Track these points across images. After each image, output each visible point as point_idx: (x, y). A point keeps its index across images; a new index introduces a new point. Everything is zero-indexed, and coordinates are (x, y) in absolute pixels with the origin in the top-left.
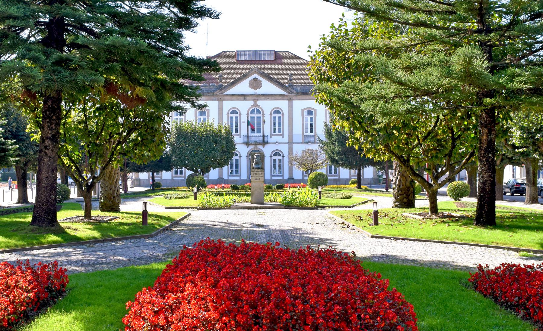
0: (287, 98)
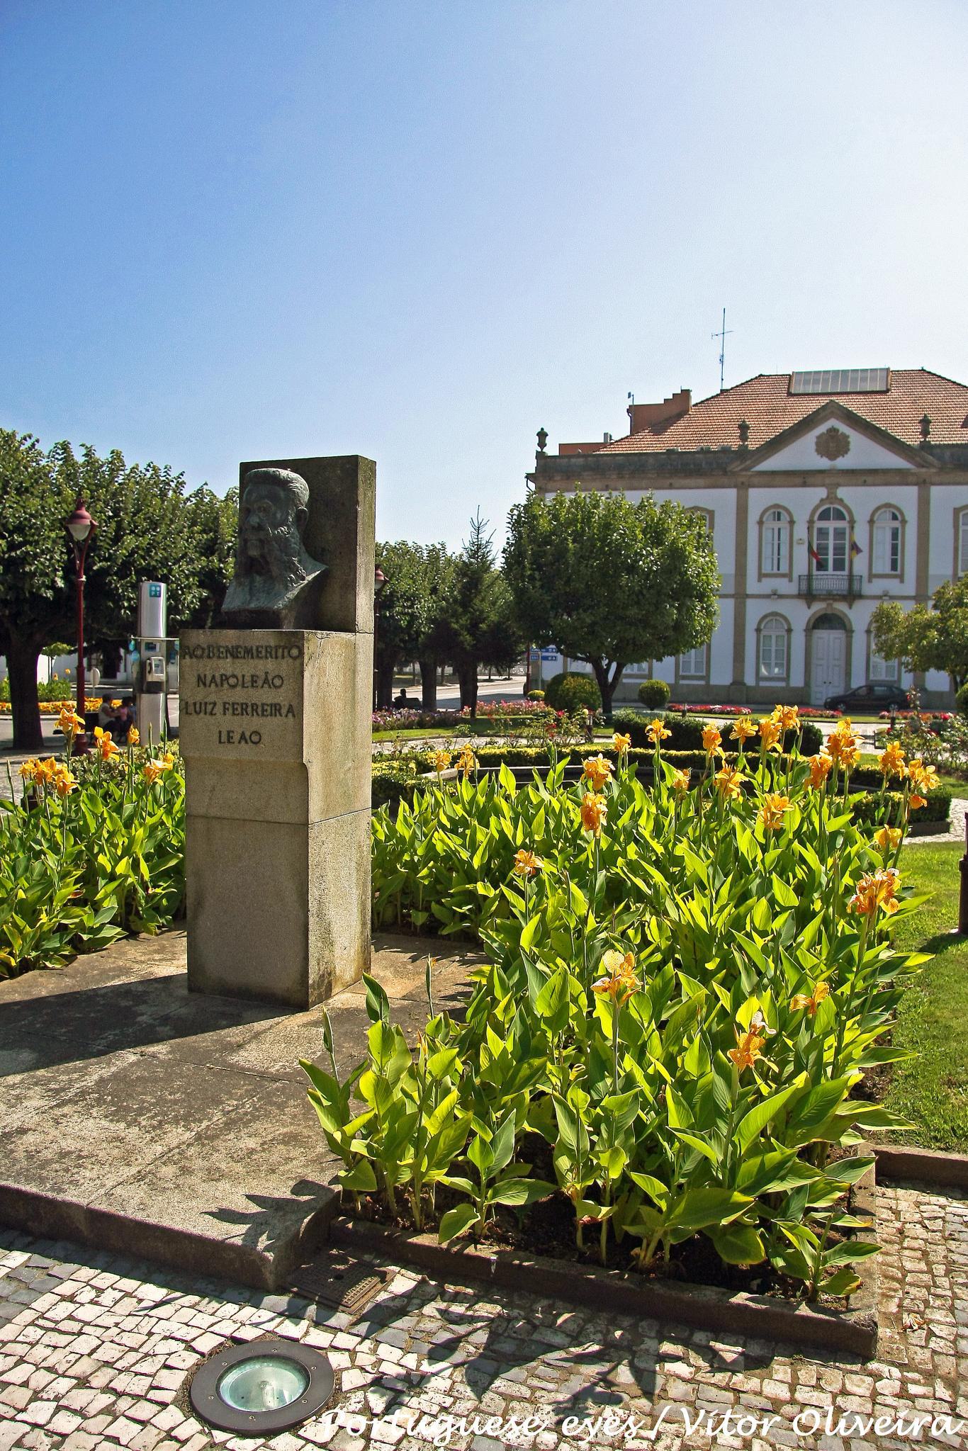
0: (913, 479)
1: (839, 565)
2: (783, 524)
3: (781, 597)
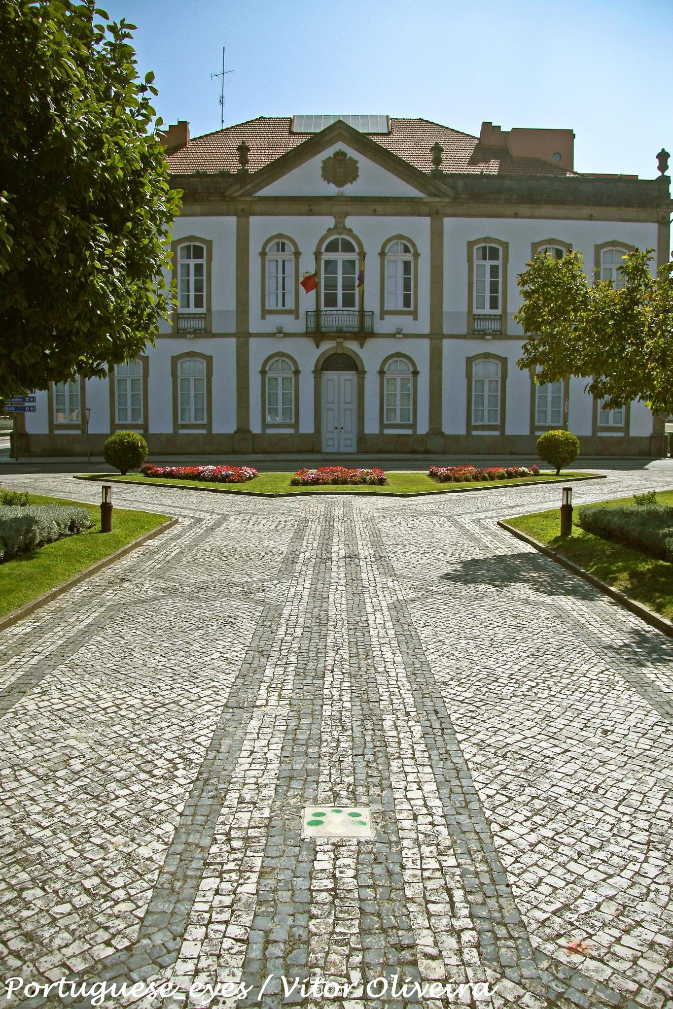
0: (425, 209)
1: (348, 301)
2: (288, 255)
3: (287, 335)
